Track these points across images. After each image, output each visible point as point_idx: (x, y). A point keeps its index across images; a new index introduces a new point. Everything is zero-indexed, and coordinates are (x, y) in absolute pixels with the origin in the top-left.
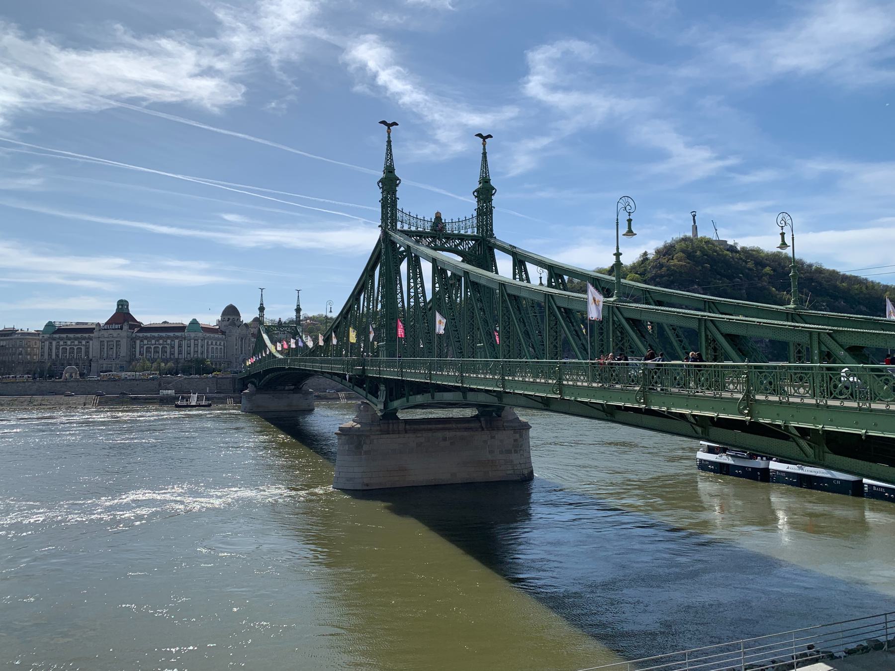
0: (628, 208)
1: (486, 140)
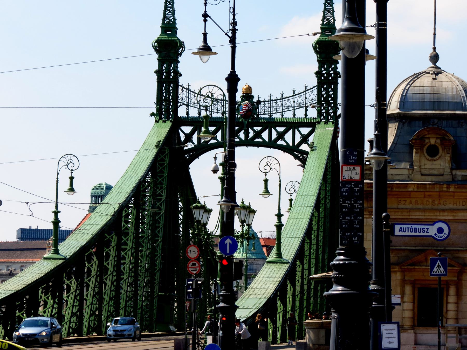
0: (70, 165)
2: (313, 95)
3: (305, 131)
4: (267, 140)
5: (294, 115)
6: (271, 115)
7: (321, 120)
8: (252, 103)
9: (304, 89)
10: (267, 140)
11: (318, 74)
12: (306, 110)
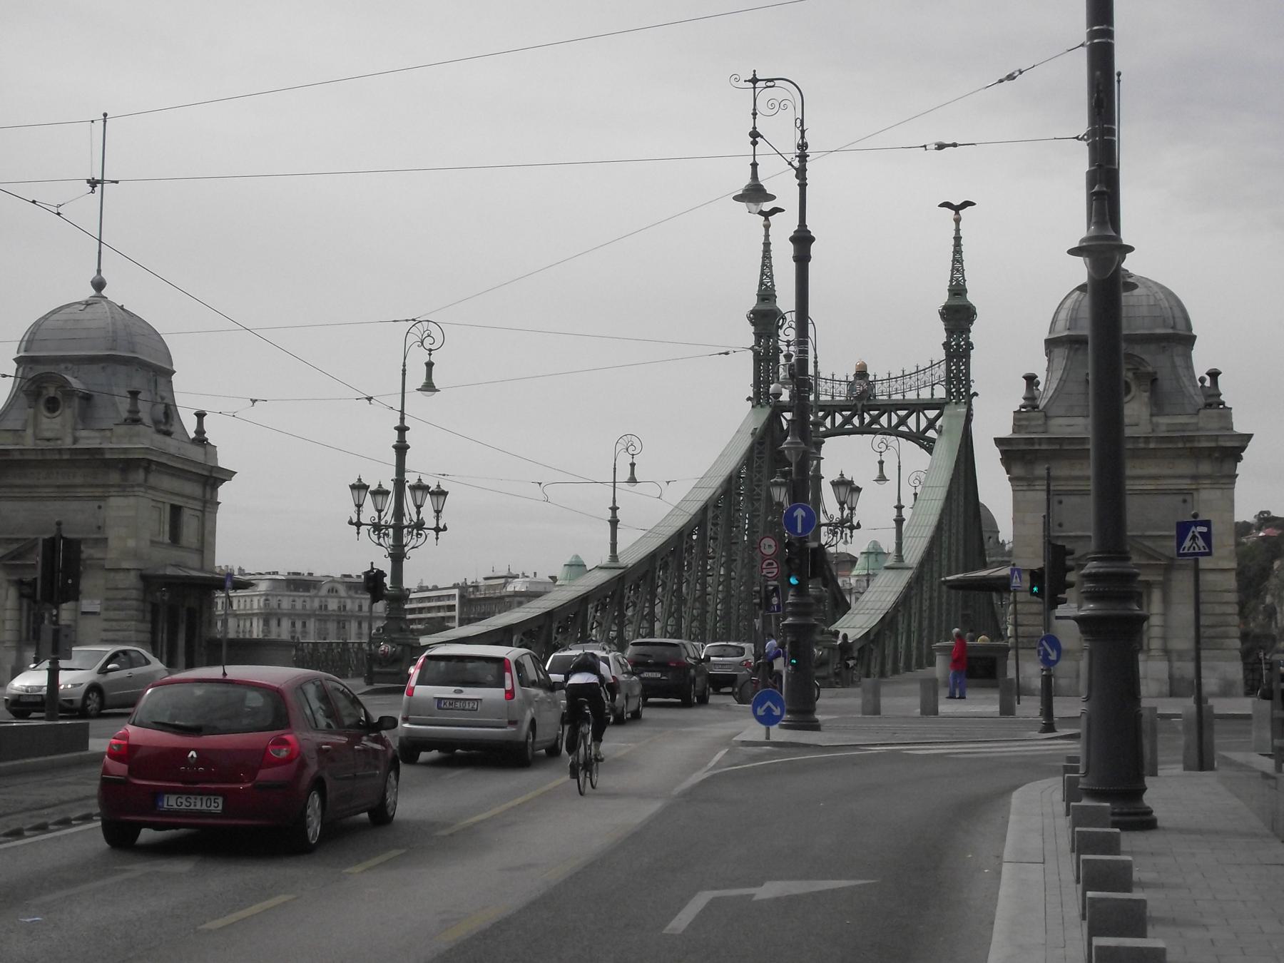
2: (941, 372)
3: (932, 414)
4: (886, 426)
5: (918, 395)
6: (890, 396)
7: (951, 400)
8: (869, 383)
9: (930, 364)
10: (886, 426)
11: (946, 346)
12: (933, 389)
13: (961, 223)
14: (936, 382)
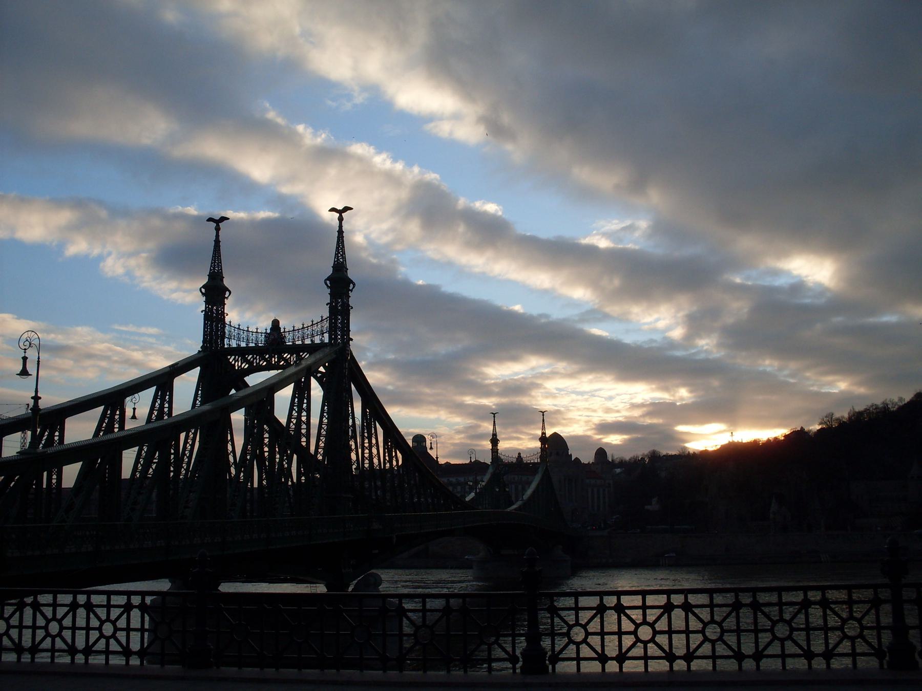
1: (343, 214)
13: (343, 222)
14: (325, 331)
